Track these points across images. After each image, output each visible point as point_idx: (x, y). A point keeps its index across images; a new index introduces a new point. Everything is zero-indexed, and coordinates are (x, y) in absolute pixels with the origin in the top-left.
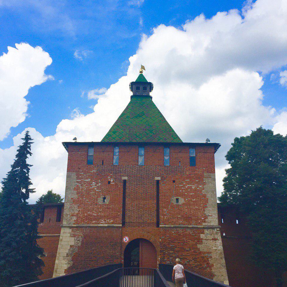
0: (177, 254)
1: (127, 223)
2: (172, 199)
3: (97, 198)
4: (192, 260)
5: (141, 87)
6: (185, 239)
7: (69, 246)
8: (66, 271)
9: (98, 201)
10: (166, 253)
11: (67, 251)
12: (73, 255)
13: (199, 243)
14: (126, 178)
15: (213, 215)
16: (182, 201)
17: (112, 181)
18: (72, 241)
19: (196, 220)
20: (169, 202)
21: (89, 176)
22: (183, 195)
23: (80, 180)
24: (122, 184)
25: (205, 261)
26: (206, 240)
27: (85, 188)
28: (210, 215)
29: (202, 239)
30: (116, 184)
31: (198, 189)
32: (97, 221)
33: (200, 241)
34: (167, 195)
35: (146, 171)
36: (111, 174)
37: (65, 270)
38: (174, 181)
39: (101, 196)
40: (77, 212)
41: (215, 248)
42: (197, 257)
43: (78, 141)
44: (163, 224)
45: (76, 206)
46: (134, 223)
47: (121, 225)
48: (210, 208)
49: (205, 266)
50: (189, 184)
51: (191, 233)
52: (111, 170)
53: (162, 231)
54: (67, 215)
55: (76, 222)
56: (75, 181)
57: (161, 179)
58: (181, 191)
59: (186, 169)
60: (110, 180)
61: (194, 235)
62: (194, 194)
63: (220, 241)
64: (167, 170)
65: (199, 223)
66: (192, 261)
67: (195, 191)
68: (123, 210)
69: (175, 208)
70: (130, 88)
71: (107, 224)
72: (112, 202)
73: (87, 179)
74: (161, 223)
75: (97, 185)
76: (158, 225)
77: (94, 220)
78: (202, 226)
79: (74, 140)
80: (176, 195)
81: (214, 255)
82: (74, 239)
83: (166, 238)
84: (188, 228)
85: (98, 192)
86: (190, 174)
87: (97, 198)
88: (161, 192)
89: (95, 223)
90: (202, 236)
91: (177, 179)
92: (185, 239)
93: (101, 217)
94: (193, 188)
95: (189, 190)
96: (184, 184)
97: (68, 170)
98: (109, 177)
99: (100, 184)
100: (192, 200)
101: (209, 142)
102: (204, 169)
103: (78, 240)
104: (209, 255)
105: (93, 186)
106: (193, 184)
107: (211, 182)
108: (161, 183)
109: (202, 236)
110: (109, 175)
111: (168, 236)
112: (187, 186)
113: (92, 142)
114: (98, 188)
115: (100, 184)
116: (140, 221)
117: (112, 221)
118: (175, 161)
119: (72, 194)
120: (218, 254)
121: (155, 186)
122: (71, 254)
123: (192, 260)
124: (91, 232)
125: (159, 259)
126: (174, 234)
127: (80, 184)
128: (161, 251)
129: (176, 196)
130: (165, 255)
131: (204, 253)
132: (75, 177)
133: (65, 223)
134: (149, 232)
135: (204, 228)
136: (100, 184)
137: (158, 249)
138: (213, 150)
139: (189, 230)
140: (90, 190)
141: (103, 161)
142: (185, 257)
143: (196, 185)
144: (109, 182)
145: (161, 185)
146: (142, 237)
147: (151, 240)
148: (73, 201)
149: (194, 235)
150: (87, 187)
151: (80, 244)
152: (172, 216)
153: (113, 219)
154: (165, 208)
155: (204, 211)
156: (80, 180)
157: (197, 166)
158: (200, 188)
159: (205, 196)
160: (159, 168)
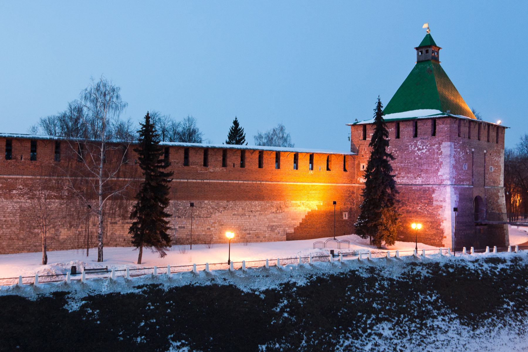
14: (473, 150)
16: (493, 170)
63: (504, 198)
144: (467, 152)
151: (458, 200)
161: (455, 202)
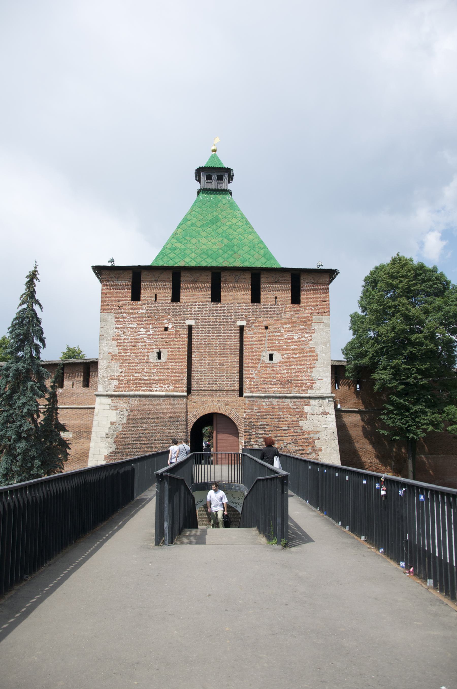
0: (270, 435)
1: (194, 390)
2: (264, 354)
3: (148, 352)
4: (291, 442)
5: (214, 177)
6: (281, 413)
7: (110, 423)
8: (106, 457)
9: (150, 357)
10: (254, 433)
11: (107, 430)
12: (115, 436)
13: (302, 418)
14: (192, 322)
15: (324, 379)
16: (277, 357)
17: (170, 327)
18: (113, 416)
19: (298, 386)
20: (259, 359)
21: (135, 318)
22: (280, 349)
23: (121, 326)
24: (186, 332)
25: (309, 444)
26: (312, 414)
27: (129, 338)
28: (320, 378)
29: (306, 413)
30: (177, 332)
31: (303, 339)
32: (149, 388)
33: (303, 415)
34: (256, 349)
35: (224, 312)
36: (169, 317)
37: (105, 456)
38: (266, 328)
39: (154, 350)
40: (119, 373)
41: (326, 426)
42: (297, 439)
43: (117, 264)
44: (249, 391)
45: (116, 365)
46: (205, 390)
47: (185, 394)
48: (320, 369)
49: (310, 450)
50: (289, 332)
51: (290, 405)
52: (169, 310)
53: (248, 402)
54: (103, 378)
55: (118, 388)
56: (114, 326)
57: (247, 324)
58: (277, 342)
59: (285, 309)
60: (166, 325)
61: (295, 407)
62: (296, 347)
64: (256, 311)
65: (304, 390)
66: (290, 444)
67: (299, 342)
68: (188, 371)
69: (268, 369)
70: (196, 176)
71: (164, 392)
72: (170, 359)
73: (132, 323)
74: (245, 390)
75: (148, 333)
76: (241, 395)
77: (146, 385)
78: (307, 395)
79: (109, 262)
80: (269, 348)
81: (322, 435)
82: (116, 413)
83: (253, 413)
84: (286, 397)
85: (149, 344)
86: (292, 317)
87: (148, 352)
88: (245, 343)
89: (147, 390)
90: (307, 409)
91: (270, 324)
92: (281, 413)
93: (155, 382)
94: (296, 338)
95: (289, 341)
96: (282, 333)
97: (103, 310)
98: (166, 321)
99: (151, 332)
100: (294, 356)
101: (321, 268)
102: (313, 308)
103: (122, 415)
104: (315, 436)
105: (142, 334)
106: (296, 333)
107: (323, 329)
108: (247, 331)
109: (307, 409)
110: (165, 318)
111: (256, 410)
112: (286, 336)
113: (139, 266)
114: (149, 337)
115: (153, 331)
116: (215, 387)
117: (171, 387)
118: (268, 296)
119: (111, 346)
120: (329, 433)
121: (238, 335)
122: (113, 435)
123: (291, 442)
124: (140, 404)
125: (243, 441)
126: (265, 407)
127: (121, 331)
128: (245, 431)
129: (270, 351)
130: (251, 436)
131: (309, 433)
132: (114, 320)
133: (101, 390)
134: (227, 404)
135: (310, 398)
136: (153, 331)
137: (241, 428)
138: (328, 280)
139: (287, 401)
140: (137, 341)
141: (156, 295)
142: (279, 438)
143: (300, 334)
144: (166, 329)
145: (246, 333)
146: (216, 411)
147: (231, 416)
148: (112, 357)
149: (295, 407)
150: (132, 335)
151: (125, 421)
152: (263, 380)
153: (173, 385)
154: (252, 368)
155: (311, 372)
156: (121, 326)
157: (302, 304)
158: (306, 338)
159: (312, 350)
160: (244, 306)
161: (109, 425)
